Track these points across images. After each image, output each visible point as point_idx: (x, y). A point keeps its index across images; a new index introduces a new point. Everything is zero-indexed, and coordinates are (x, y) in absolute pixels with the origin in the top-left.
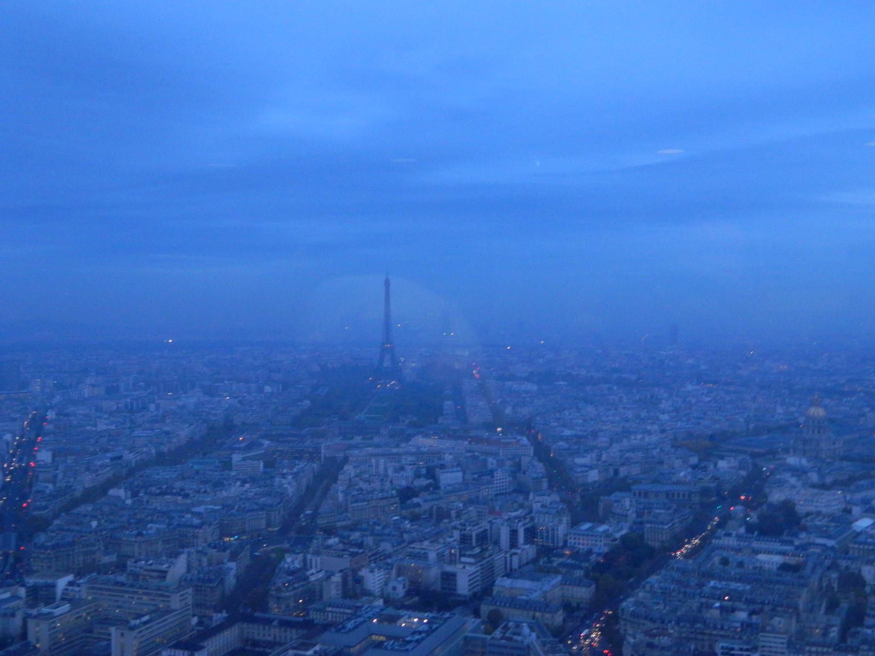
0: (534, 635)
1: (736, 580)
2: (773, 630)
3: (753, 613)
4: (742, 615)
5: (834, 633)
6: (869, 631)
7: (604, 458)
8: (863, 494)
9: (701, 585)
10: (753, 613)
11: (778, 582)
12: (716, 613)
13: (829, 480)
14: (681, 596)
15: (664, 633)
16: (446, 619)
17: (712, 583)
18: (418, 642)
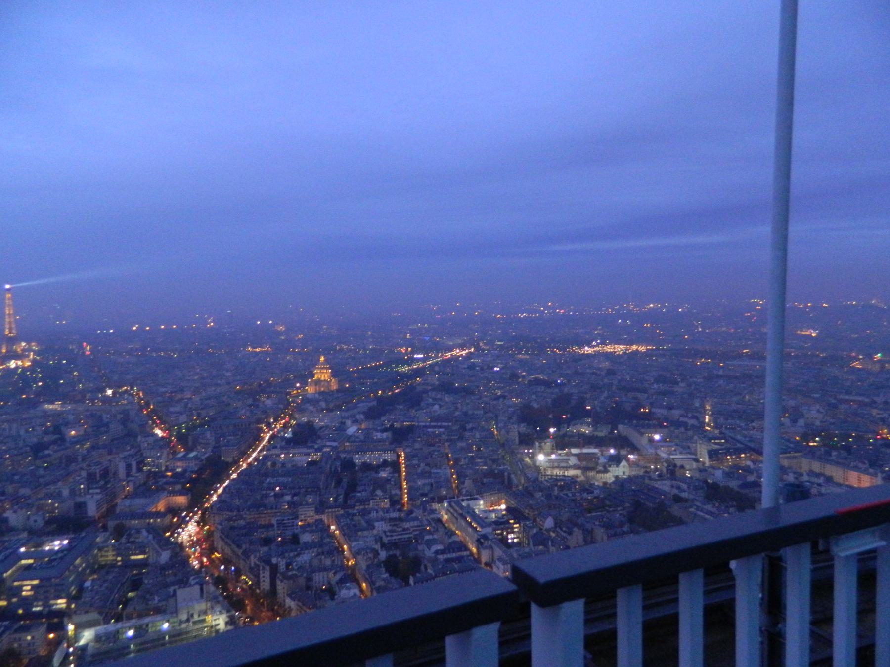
0: (151, 536)
1: (282, 476)
2: (307, 504)
3: (294, 495)
4: (288, 498)
5: (341, 500)
6: (359, 494)
7: (189, 405)
8: (351, 412)
9: (261, 482)
10: (292, 497)
11: (308, 473)
12: (272, 498)
13: (331, 406)
14: (249, 492)
15: (241, 518)
16: (83, 538)
17: (268, 480)
18: (61, 558)
